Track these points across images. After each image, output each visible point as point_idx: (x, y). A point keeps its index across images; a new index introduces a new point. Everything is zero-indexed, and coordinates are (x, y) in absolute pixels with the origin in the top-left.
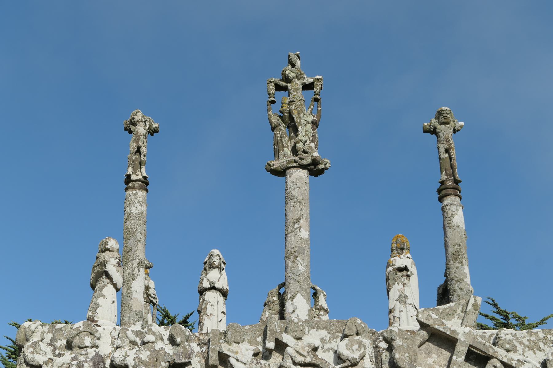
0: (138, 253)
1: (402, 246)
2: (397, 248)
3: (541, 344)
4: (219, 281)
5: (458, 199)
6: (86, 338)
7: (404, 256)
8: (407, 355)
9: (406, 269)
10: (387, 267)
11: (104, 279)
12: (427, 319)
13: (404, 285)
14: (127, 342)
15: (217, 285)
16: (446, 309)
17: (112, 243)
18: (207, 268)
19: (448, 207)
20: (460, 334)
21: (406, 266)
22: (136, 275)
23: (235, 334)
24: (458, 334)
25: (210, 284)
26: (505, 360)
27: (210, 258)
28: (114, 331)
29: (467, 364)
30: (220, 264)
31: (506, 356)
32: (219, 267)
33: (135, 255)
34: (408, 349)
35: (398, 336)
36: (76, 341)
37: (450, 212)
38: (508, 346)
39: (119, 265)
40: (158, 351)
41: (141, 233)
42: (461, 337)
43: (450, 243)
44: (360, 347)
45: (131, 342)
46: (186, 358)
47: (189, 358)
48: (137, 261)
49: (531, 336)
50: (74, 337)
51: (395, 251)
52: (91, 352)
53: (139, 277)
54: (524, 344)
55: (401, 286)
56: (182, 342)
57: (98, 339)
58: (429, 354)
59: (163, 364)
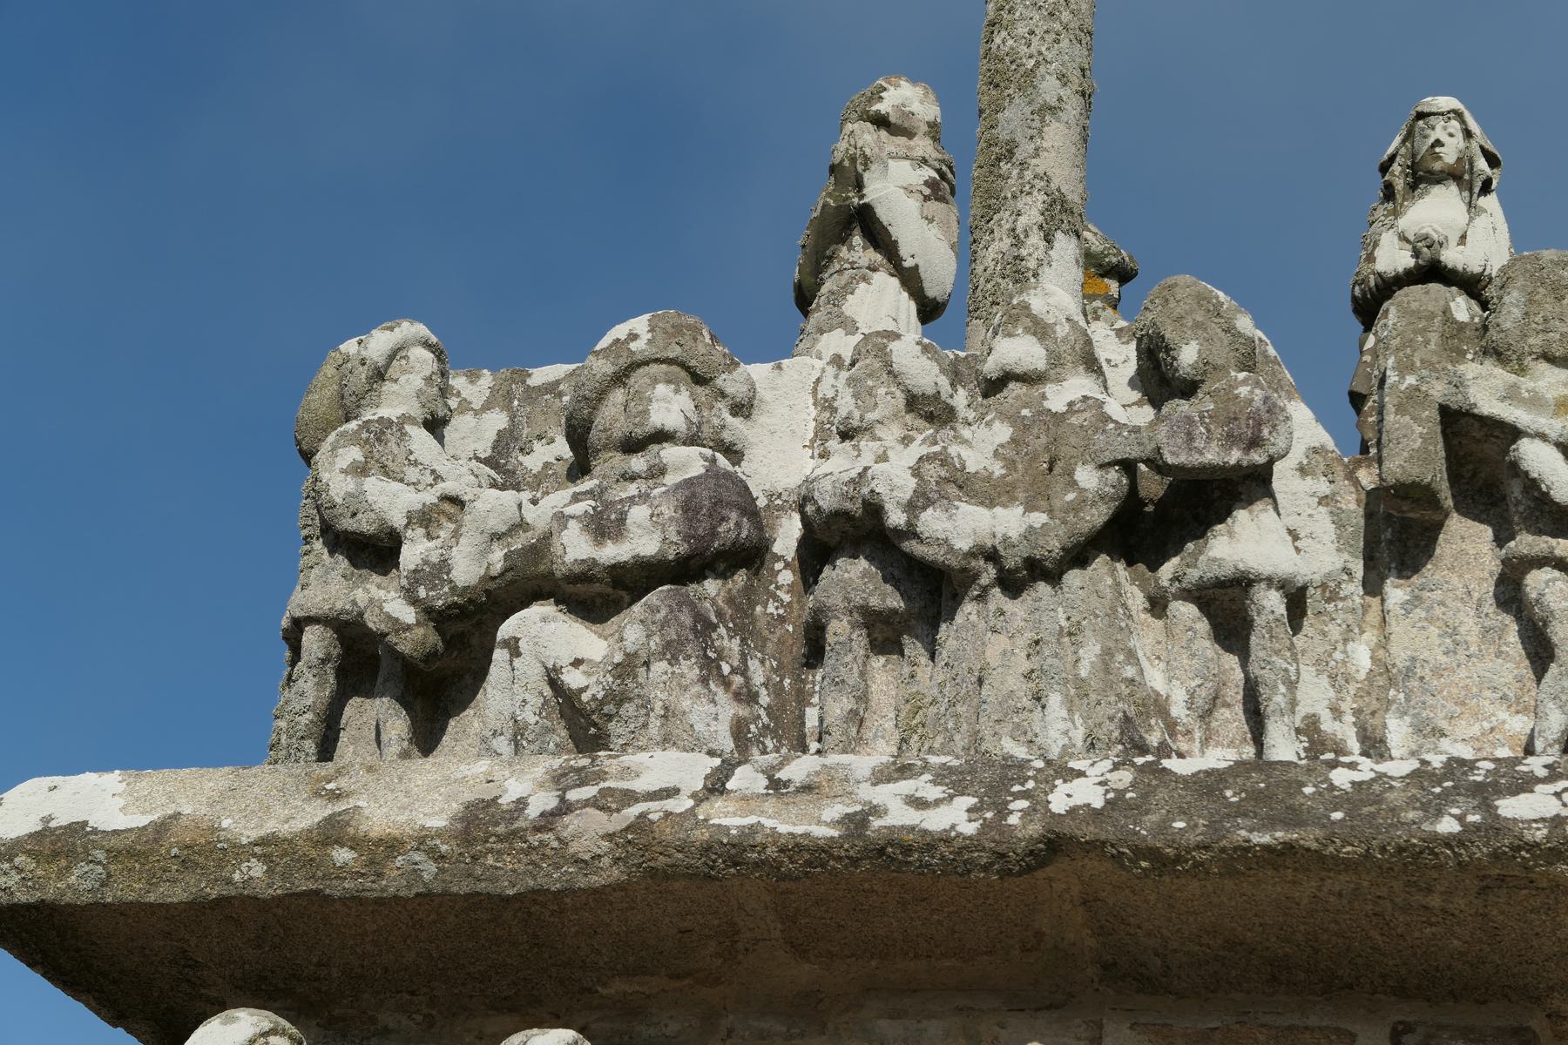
0: (1041, 164)
4: (1463, 239)
6: (661, 389)
11: (858, 251)
14: (889, 400)
15: (1452, 257)
17: (904, 96)
18: (1399, 184)
22: (1032, 264)
23: (1549, 307)
25: (1417, 254)
27: (1409, 136)
28: (831, 370)
30: (1465, 160)
32: (1457, 175)
33: (1028, 175)
36: (612, 416)
39: (939, 189)
40: (1059, 418)
41: (1063, 78)
45: (914, 402)
46: (1231, 440)
47: (1255, 442)
48: (1042, 197)
50: (601, 395)
52: (686, 462)
53: (1046, 272)
56: (1207, 366)
57: (742, 409)
59: (1087, 477)
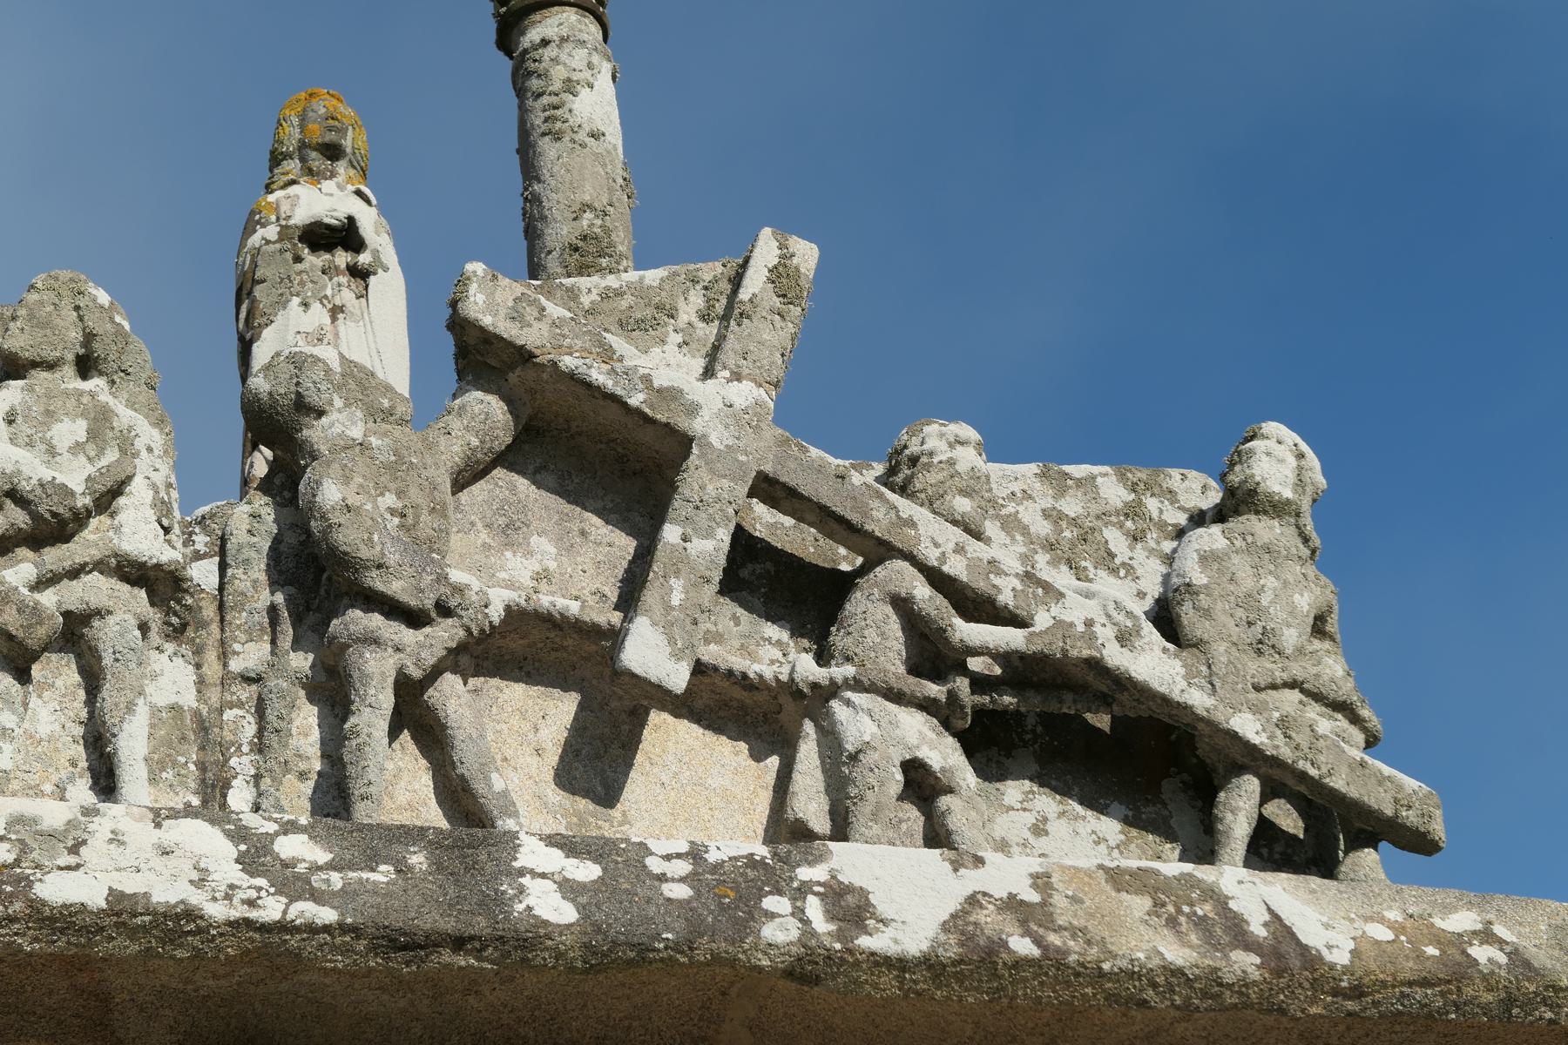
1: (331, 137)
2: (303, 146)
3: (1115, 539)
5: (592, 30)
7: (341, 187)
8: (390, 500)
9: (345, 236)
10: (249, 230)
12: (516, 317)
13: (336, 311)
16: (619, 293)
19: (548, 53)
20: (705, 413)
21: (351, 219)
24: (693, 410)
26: (955, 567)
29: (729, 607)
31: (960, 549)
34: (396, 470)
35: (339, 388)
37: (558, 74)
38: (963, 505)
42: (709, 427)
43: (556, 202)
44: (93, 435)
49: (1061, 492)
51: (293, 166)
54: (1025, 531)
55: (318, 315)
58: (510, 531)
